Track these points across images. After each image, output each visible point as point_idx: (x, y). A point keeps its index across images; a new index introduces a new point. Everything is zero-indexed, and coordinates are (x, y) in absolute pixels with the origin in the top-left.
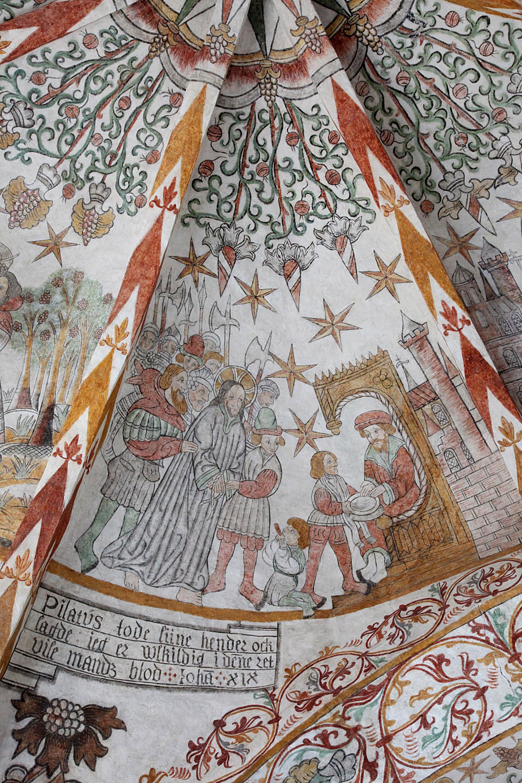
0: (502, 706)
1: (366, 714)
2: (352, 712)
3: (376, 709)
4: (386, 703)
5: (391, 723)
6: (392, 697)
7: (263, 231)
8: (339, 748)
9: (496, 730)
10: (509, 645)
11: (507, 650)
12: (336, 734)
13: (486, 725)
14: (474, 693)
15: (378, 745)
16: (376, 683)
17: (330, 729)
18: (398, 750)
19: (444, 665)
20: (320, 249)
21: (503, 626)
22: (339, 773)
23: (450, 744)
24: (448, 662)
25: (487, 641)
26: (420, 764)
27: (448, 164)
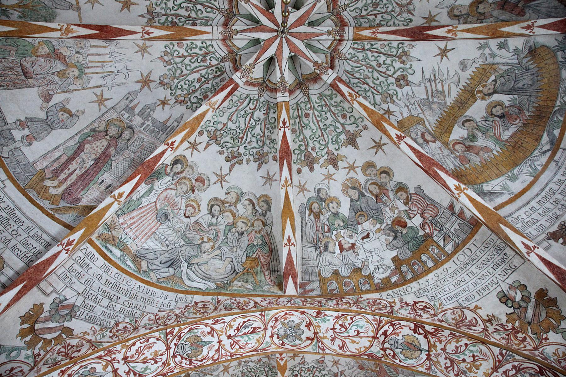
0: (329, 320)
1: (376, 351)
2: (380, 355)
3: (372, 349)
4: (367, 349)
5: (369, 341)
6: (364, 349)
7: (324, 373)
8: (391, 350)
9: (336, 314)
10: (315, 338)
11: (317, 337)
12: (389, 354)
13: (338, 317)
14: (336, 330)
15: (378, 338)
16: (366, 357)
17: (390, 357)
18: (373, 332)
19: (341, 346)
20: (309, 362)
21: (314, 345)
22: (397, 343)
23: (354, 320)
24: (339, 346)
25: (322, 343)
26: (368, 321)
27: (262, 369)
